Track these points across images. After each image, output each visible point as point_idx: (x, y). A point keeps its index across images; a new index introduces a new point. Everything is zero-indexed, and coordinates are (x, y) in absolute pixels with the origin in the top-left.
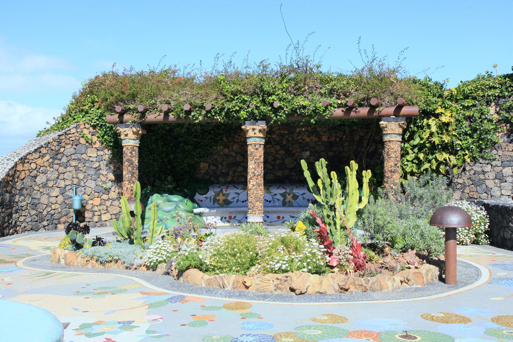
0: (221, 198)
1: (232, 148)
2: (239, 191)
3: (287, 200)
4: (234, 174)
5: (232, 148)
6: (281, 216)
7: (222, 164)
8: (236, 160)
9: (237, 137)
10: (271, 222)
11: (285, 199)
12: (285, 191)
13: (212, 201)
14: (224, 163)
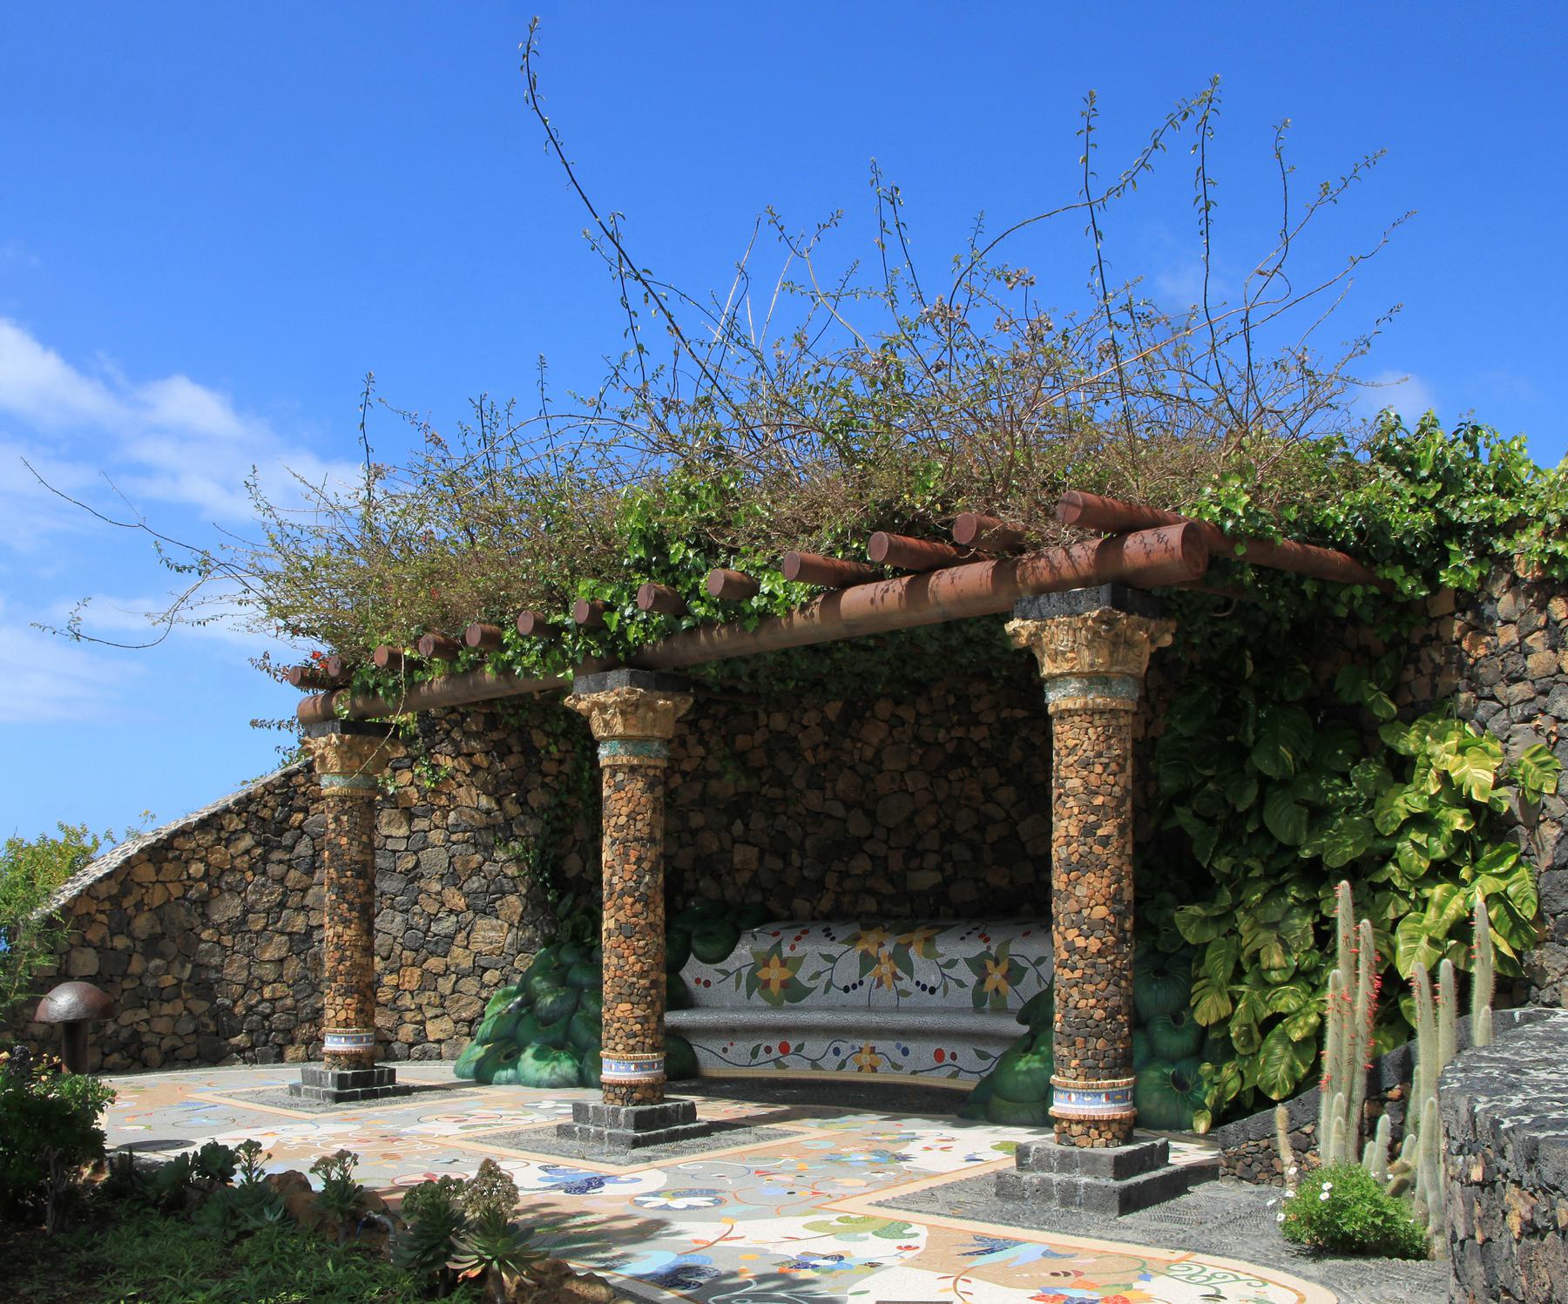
0: (775, 974)
1: (833, 789)
2: (834, 949)
3: (989, 986)
4: (839, 884)
5: (833, 789)
7: (801, 848)
9: (847, 744)
10: (914, 1073)
11: (982, 982)
13: (744, 983)
14: (808, 843)
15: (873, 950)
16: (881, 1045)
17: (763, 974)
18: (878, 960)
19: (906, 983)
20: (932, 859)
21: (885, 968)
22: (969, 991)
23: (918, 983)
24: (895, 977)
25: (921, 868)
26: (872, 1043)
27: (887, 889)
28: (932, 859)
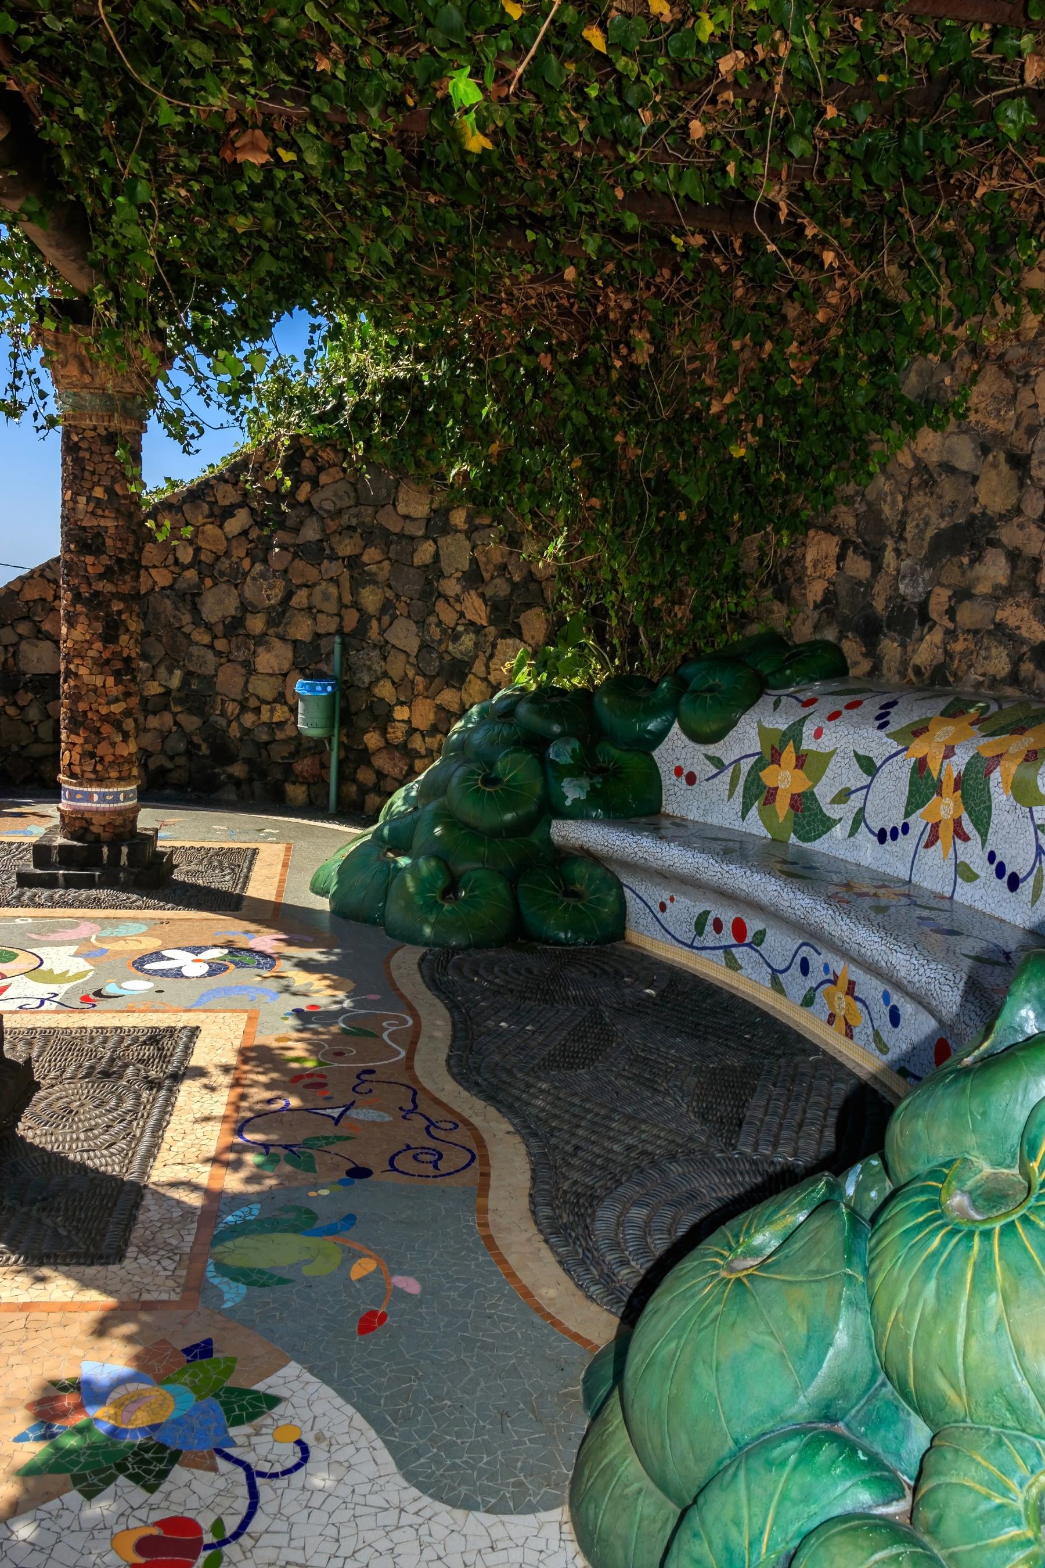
13: (740, 789)
17: (770, 776)
23: (992, 857)
24: (960, 834)
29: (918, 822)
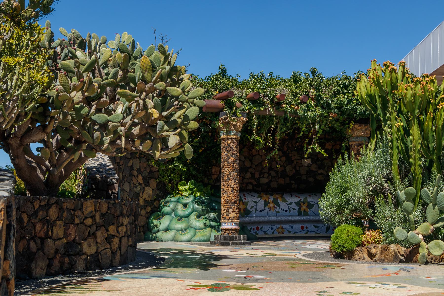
3: (302, 210)
6: (305, 226)
8: (245, 165)
11: (300, 208)
12: (299, 199)
15: (267, 200)
16: (285, 226)
18: (269, 203)
19: (278, 209)
20: (266, 175)
21: (272, 205)
22: (297, 211)
23: (282, 209)
24: (275, 207)
25: (263, 177)
26: (282, 225)
27: (255, 183)
28: (266, 175)
29: (267, 208)
